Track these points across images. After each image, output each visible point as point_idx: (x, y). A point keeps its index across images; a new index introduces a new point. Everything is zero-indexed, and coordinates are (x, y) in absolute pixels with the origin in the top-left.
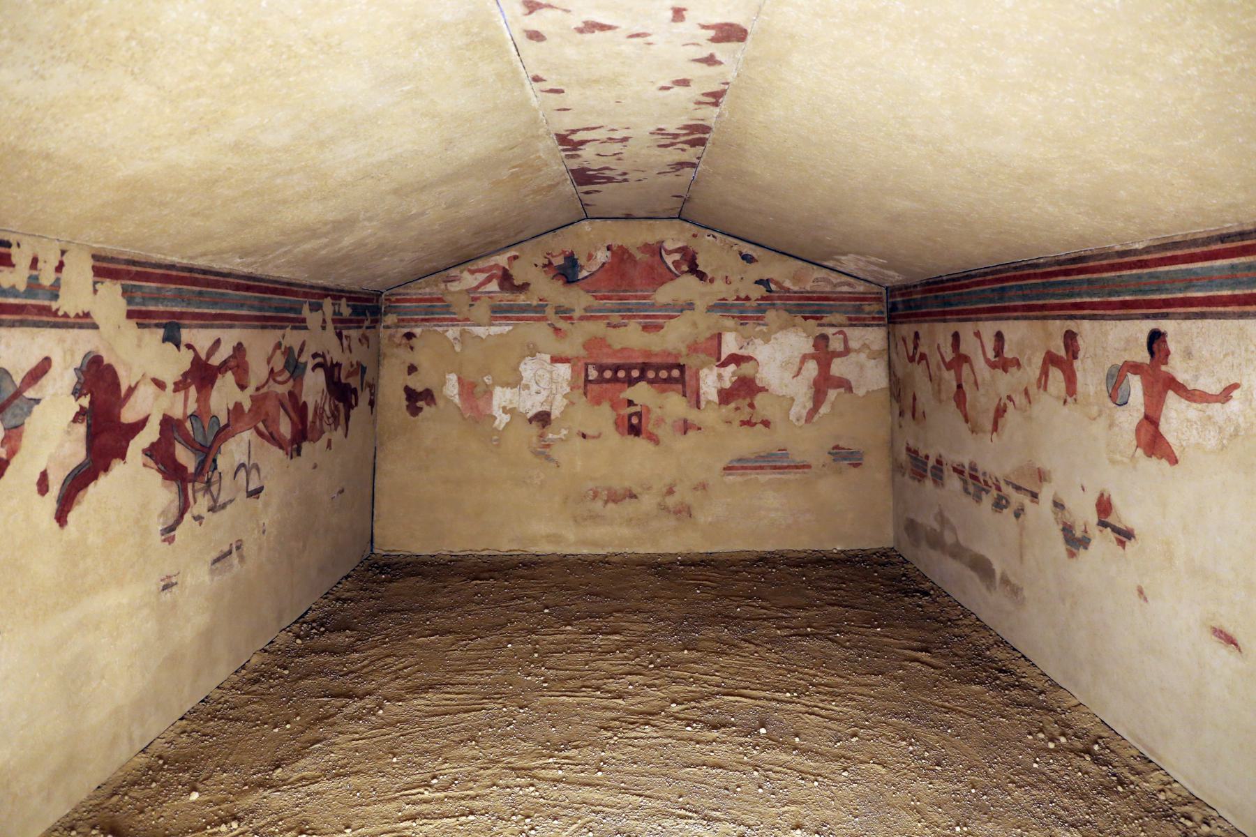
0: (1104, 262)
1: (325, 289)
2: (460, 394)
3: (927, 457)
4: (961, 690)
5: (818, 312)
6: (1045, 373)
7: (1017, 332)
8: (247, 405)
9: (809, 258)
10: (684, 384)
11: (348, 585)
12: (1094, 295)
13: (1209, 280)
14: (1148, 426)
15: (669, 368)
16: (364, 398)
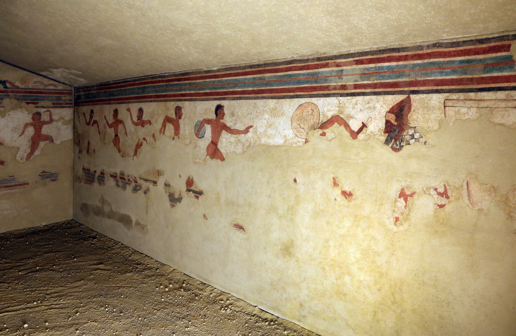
0: (198, 75)
3: (95, 172)
4: (122, 277)
5: (35, 100)
6: (164, 126)
7: (150, 108)
9: (31, 70)
12: (192, 90)
13: (244, 83)
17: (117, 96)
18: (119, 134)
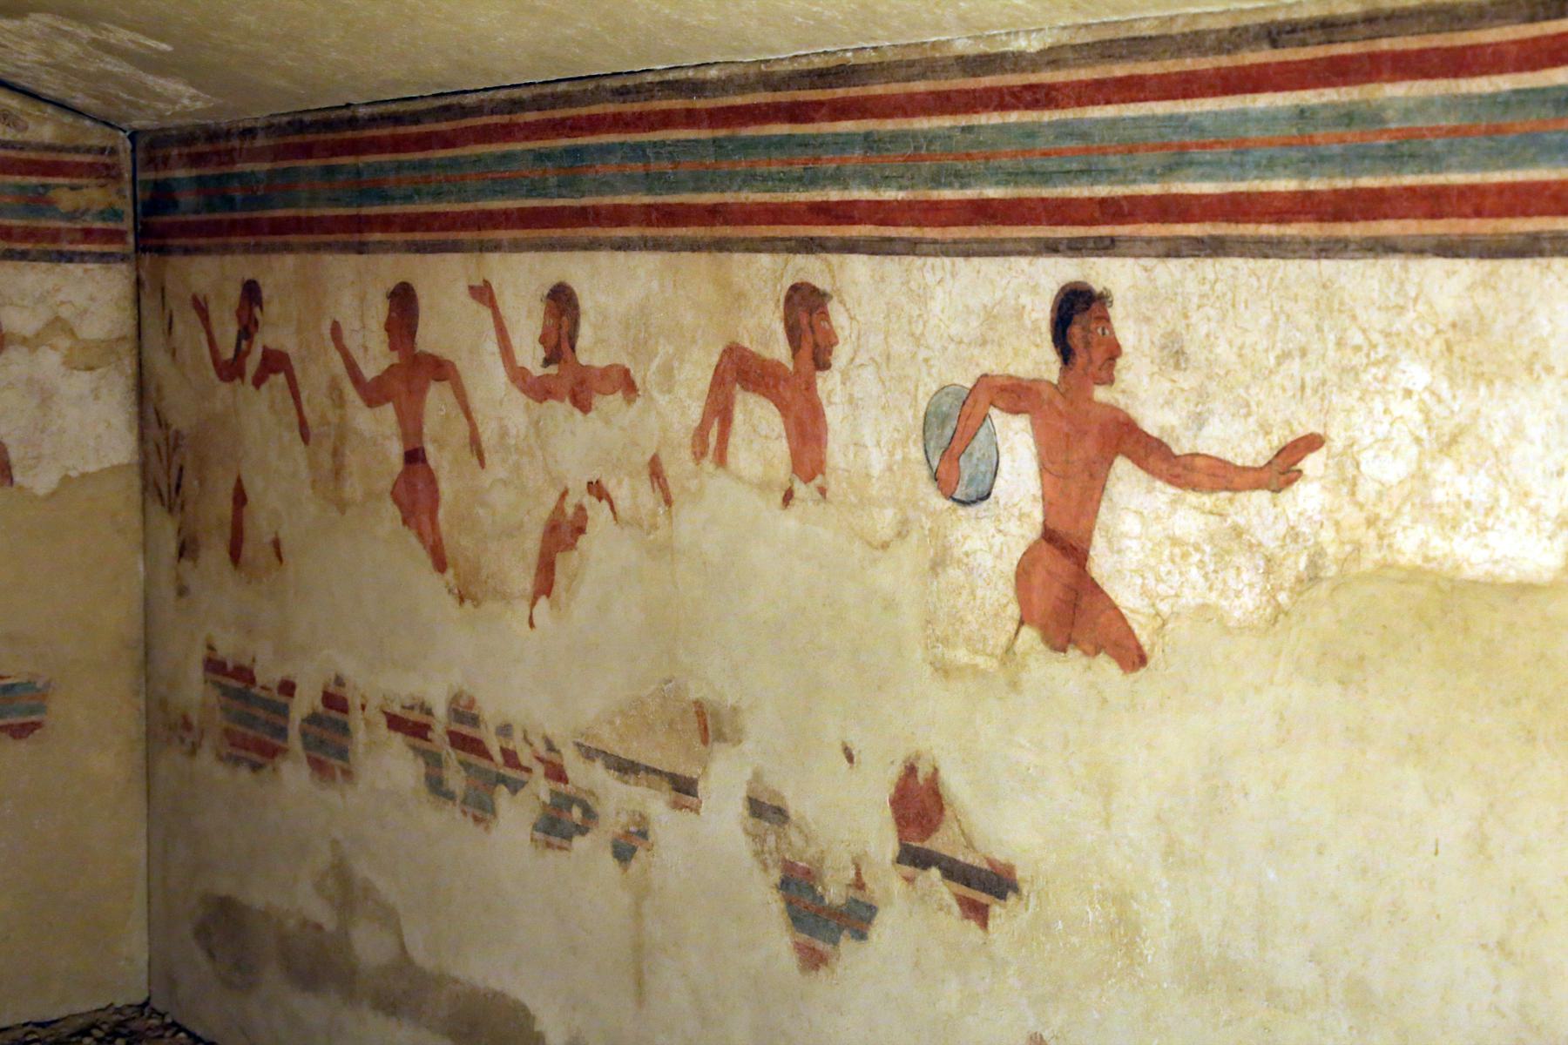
0: (920, 86)
3: (288, 688)
6: (720, 411)
7: (627, 292)
12: (886, 181)
13: (1235, 147)
14: (1063, 566)
17: (408, 198)
18: (430, 450)
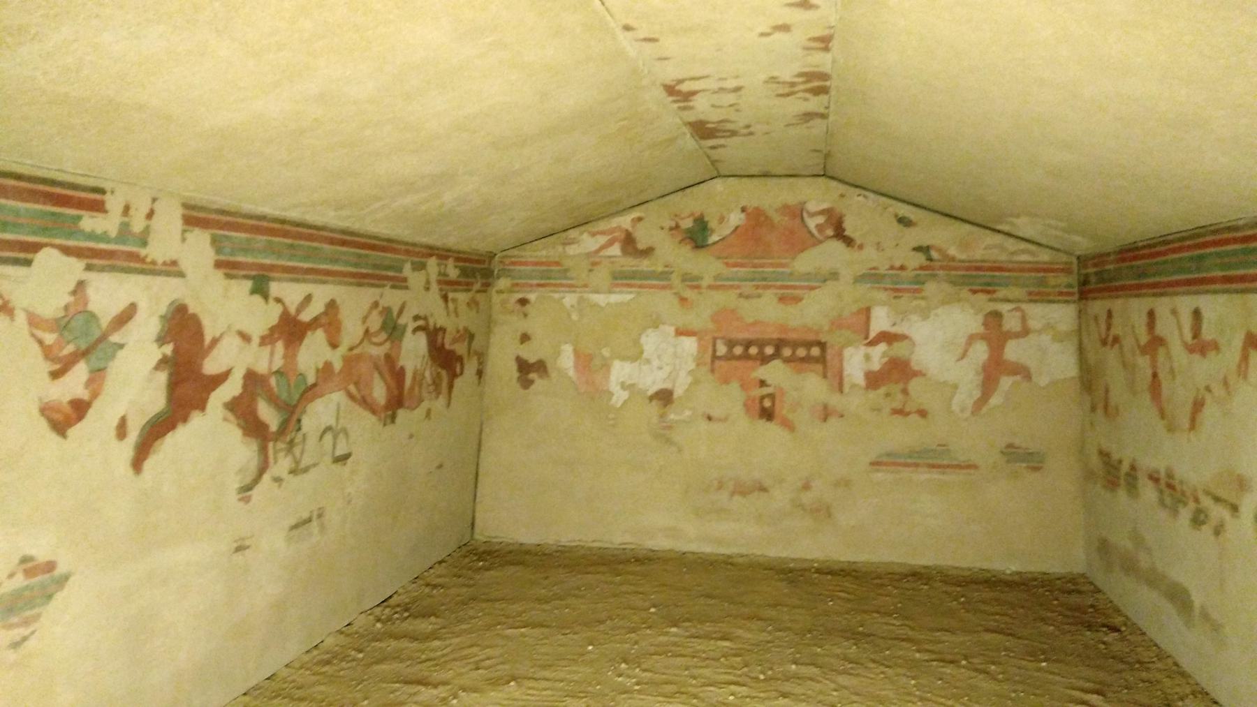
1: (431, 248)
2: (576, 366)
3: (1120, 462)
5: (989, 284)
7: (1218, 309)
8: (338, 366)
9: (979, 220)
10: (825, 367)
11: (440, 570)
15: (808, 345)
16: (471, 367)
